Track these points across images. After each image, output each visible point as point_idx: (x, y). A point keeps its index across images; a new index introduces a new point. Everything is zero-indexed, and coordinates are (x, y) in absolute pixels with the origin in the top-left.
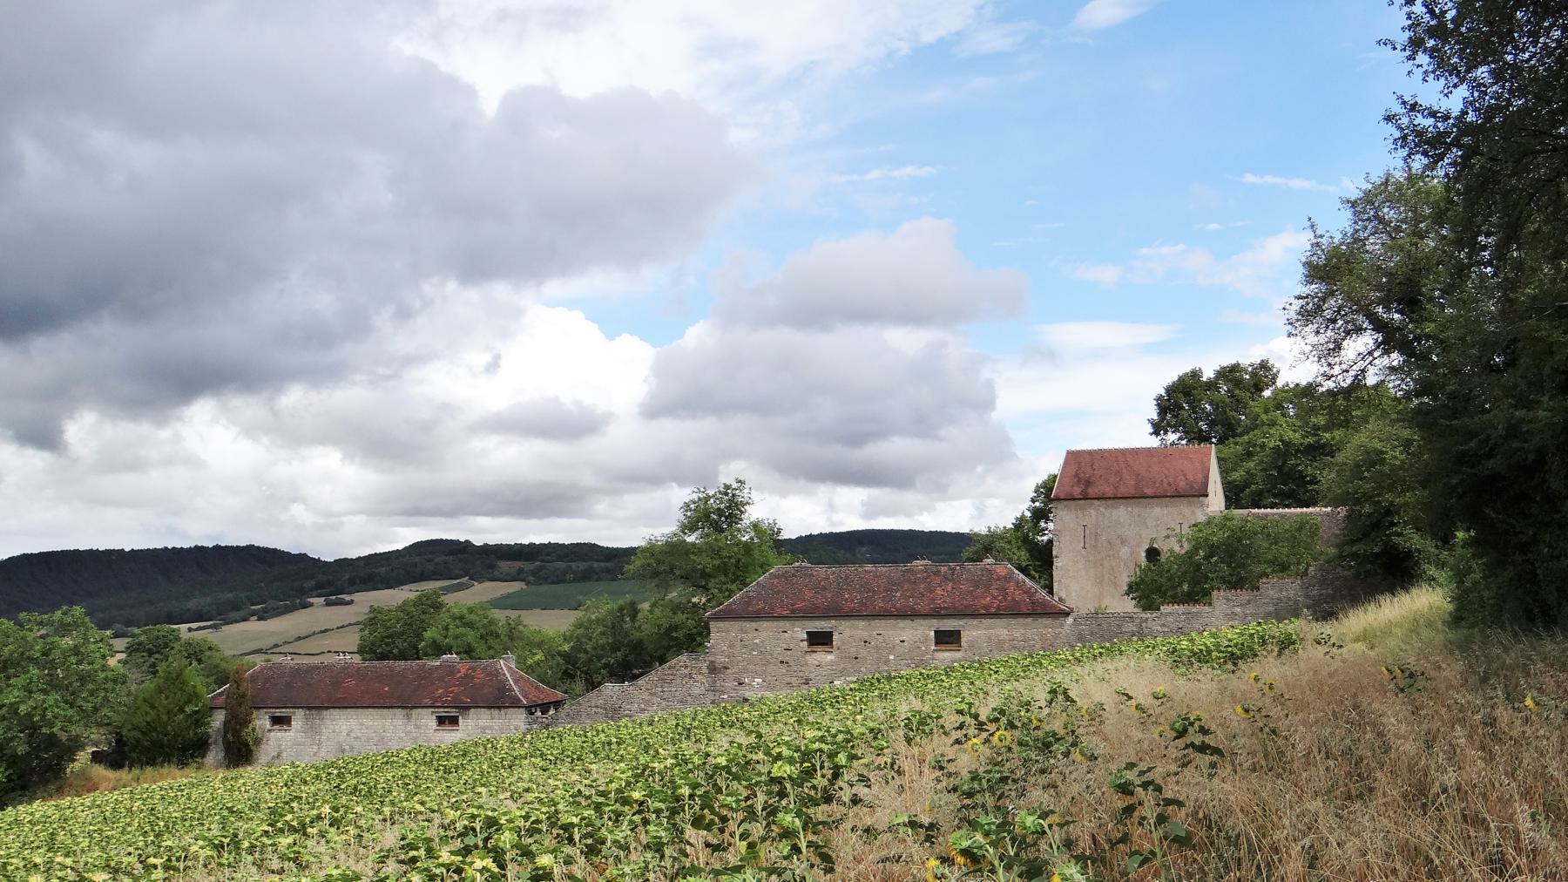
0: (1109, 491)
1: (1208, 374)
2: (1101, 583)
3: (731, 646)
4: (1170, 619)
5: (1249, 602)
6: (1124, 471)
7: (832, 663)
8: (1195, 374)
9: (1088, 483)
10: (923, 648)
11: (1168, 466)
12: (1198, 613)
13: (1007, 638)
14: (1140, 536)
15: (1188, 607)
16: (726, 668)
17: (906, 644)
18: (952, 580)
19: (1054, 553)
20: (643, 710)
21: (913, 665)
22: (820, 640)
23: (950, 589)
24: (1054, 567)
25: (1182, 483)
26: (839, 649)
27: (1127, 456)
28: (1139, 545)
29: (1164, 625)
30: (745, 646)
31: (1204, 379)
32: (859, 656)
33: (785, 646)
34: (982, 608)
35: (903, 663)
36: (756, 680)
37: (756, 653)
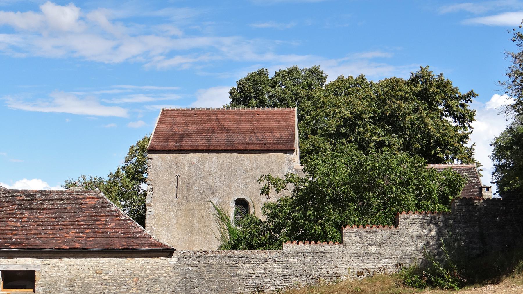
0: (202, 145)
1: (271, 75)
2: (191, 231)
4: (294, 260)
5: (385, 241)
6: (216, 127)
8: (262, 73)
11: (256, 124)
13: (95, 281)
14: (230, 187)
15: (316, 246)
18: (31, 209)
19: (147, 202)
23: (25, 219)
24: (147, 216)
25: (270, 139)
29: (286, 267)
31: (270, 78)
34: (64, 243)
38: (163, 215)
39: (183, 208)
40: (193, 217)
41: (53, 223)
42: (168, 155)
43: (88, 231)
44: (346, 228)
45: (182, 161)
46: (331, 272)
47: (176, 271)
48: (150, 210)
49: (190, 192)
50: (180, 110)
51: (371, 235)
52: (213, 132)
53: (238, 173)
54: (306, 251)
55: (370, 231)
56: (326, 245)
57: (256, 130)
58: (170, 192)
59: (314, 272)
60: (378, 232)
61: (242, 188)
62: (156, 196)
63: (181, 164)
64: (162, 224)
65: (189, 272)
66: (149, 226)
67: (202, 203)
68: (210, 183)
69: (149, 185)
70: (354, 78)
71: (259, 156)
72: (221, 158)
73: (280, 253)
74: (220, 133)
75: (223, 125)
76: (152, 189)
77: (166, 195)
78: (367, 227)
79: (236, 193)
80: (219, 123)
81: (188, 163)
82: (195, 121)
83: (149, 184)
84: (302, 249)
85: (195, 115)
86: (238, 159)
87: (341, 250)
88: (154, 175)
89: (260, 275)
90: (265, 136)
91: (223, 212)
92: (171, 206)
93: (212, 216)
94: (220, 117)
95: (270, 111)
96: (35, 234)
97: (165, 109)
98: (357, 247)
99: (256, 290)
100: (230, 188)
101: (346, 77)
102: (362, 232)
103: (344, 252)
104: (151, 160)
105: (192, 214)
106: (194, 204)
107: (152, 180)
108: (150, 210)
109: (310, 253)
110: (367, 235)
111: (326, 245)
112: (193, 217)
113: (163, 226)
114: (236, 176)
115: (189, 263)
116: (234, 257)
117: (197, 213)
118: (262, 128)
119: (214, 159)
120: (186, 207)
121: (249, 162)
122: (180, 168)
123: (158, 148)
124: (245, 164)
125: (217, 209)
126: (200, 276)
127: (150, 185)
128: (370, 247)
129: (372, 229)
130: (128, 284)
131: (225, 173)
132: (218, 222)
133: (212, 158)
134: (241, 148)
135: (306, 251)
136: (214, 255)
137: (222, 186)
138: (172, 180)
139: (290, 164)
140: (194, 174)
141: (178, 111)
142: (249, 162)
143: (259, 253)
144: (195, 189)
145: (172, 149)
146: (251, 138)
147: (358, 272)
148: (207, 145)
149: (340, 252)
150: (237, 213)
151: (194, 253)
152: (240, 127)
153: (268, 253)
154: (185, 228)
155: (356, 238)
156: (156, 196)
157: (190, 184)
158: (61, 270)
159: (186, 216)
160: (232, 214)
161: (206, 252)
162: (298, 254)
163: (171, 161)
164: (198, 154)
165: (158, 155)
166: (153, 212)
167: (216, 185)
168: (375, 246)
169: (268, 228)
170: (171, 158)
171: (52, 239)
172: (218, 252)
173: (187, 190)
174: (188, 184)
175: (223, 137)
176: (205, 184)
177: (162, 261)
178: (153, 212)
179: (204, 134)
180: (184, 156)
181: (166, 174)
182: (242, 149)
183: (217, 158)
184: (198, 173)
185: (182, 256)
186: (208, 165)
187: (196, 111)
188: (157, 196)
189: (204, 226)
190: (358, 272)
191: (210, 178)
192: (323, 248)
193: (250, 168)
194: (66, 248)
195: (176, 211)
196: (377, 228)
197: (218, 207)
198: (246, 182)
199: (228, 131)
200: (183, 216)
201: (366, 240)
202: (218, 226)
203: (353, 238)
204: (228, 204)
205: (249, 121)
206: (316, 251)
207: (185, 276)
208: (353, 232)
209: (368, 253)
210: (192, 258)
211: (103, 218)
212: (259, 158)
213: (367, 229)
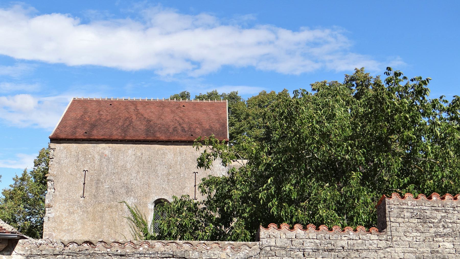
0: (116, 135)
6: (134, 117)
11: (181, 115)
12: (352, 249)
25: (197, 130)
27: (138, 105)
28: (146, 196)
38: (65, 218)
39: (90, 209)
40: (103, 221)
42: (74, 146)
44: (391, 199)
45: (92, 153)
48: (50, 212)
49: (100, 191)
50: (94, 99)
51: (443, 214)
52: (131, 122)
53: (159, 168)
54: (309, 246)
55: (440, 205)
56: (351, 233)
57: (181, 121)
58: (76, 190)
60: (456, 209)
61: (164, 186)
62: (58, 194)
63: (90, 156)
64: (64, 229)
66: (47, 231)
67: (114, 204)
68: (124, 179)
69: (50, 181)
70: (277, 93)
71: (185, 148)
72: (139, 149)
73: (255, 249)
74: (138, 123)
75: (142, 115)
76: (53, 186)
77: (70, 194)
78: (434, 198)
79: (156, 193)
81: (99, 155)
82: (109, 111)
83: (50, 180)
84: (301, 241)
85: (111, 105)
86: (159, 152)
87: (383, 244)
88: (56, 169)
90: (192, 127)
91: (140, 215)
92: (76, 207)
93: (125, 220)
94: (140, 107)
95: (197, 102)
97: (76, 99)
98: (415, 240)
100: (149, 186)
101: (268, 92)
102: (425, 208)
103: (388, 250)
104: (54, 151)
105: (101, 217)
106: (105, 205)
108: (50, 212)
109: (318, 250)
110: (435, 215)
111: (351, 233)
112: (103, 221)
113: (64, 231)
114: (155, 171)
116: (152, 256)
117: (107, 216)
118: (188, 119)
119: (130, 152)
120: (94, 209)
121: (173, 156)
122: (89, 161)
123: (63, 136)
124: (168, 158)
125: (132, 212)
127: (51, 181)
128: (440, 239)
129: (444, 201)
131: (143, 168)
132: (133, 228)
133: (128, 149)
134: (163, 138)
135: (309, 246)
136: (109, 250)
137: (139, 184)
138: (78, 176)
140: (105, 167)
141: (91, 101)
142: (173, 156)
143: (208, 248)
144: (106, 186)
145: (80, 138)
146: (175, 129)
148: (123, 135)
149: (380, 249)
150: (156, 218)
151: (63, 246)
152: (163, 117)
153: (229, 247)
154: (92, 234)
155: (412, 220)
156: (58, 194)
157: (100, 181)
159: (94, 220)
160: (150, 218)
161: (90, 243)
162: (292, 252)
163: (78, 153)
164: (111, 145)
165: (62, 145)
166: (53, 214)
167: (132, 183)
168: (451, 239)
169: (209, 219)
170: (79, 149)
172: (117, 245)
173: (97, 188)
174: (98, 180)
175: (142, 127)
176: (118, 181)
178: (53, 214)
179: (120, 124)
180: (94, 147)
181: (71, 168)
182: (165, 139)
183: (134, 150)
184: (110, 167)
185: (35, 252)
186: (123, 158)
187: (112, 101)
188: (59, 194)
189: (116, 233)
191: (125, 173)
192: (344, 240)
193: (173, 162)
195: (81, 213)
196: (455, 201)
197: (133, 209)
198: (169, 179)
199: (149, 121)
200: (91, 220)
201: (432, 225)
202: (132, 232)
203: (407, 220)
204: (145, 205)
206: (330, 247)
208: (405, 206)
209: (438, 252)
210: (58, 256)
212: (185, 151)
213: (434, 202)
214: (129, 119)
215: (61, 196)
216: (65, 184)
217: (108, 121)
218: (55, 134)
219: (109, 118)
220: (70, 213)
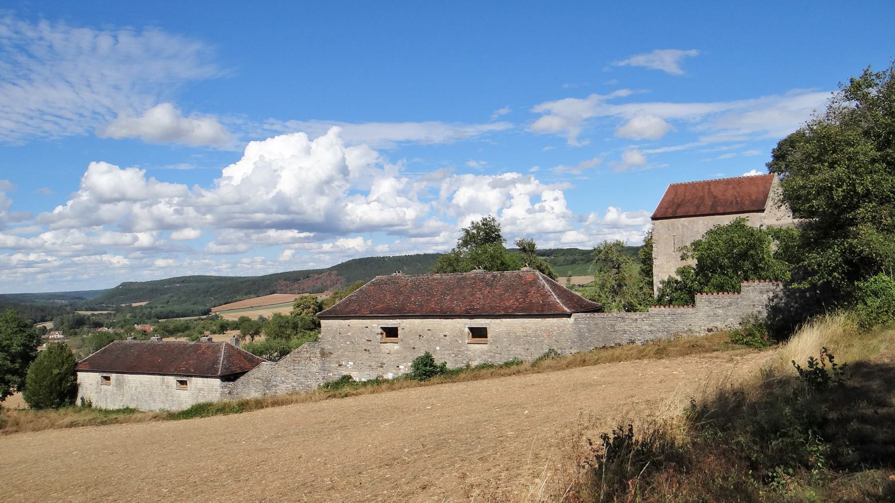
0: (692, 210)
3: (334, 337)
4: (658, 320)
5: (730, 304)
6: (706, 195)
7: (397, 352)
9: (679, 205)
10: (460, 342)
11: (739, 190)
13: (524, 334)
15: (674, 309)
16: (331, 353)
17: (447, 338)
19: (653, 256)
20: (283, 382)
21: (453, 355)
22: (391, 332)
24: (654, 266)
25: (747, 202)
26: (402, 341)
29: (651, 325)
30: (342, 337)
32: (415, 347)
33: (368, 339)
35: (446, 352)
36: (350, 363)
37: (349, 343)
41: (502, 295)
42: (666, 222)
43: (521, 300)
46: (686, 329)
47: (574, 328)
54: (666, 313)
59: (674, 328)
65: (582, 328)
75: (712, 193)
80: (710, 191)
87: (694, 312)
89: (632, 331)
96: (488, 303)
99: (630, 341)
107: (655, 240)
115: (582, 322)
119: (700, 222)
123: (658, 216)
126: (590, 331)
130: (543, 336)
134: (721, 211)
135: (666, 313)
139: (762, 221)
147: (708, 329)
152: (726, 194)
158: (502, 327)
171: (498, 306)
175: (710, 203)
177: (564, 321)
179: (696, 202)
187: (695, 184)
190: (708, 329)
194: (503, 313)
199: (716, 197)
205: (734, 188)
207: (580, 332)
211: (533, 290)
214: (702, 198)
215: (661, 252)
216: (663, 245)
217: (689, 200)
218: (653, 215)
219: (690, 198)
220: (668, 262)
